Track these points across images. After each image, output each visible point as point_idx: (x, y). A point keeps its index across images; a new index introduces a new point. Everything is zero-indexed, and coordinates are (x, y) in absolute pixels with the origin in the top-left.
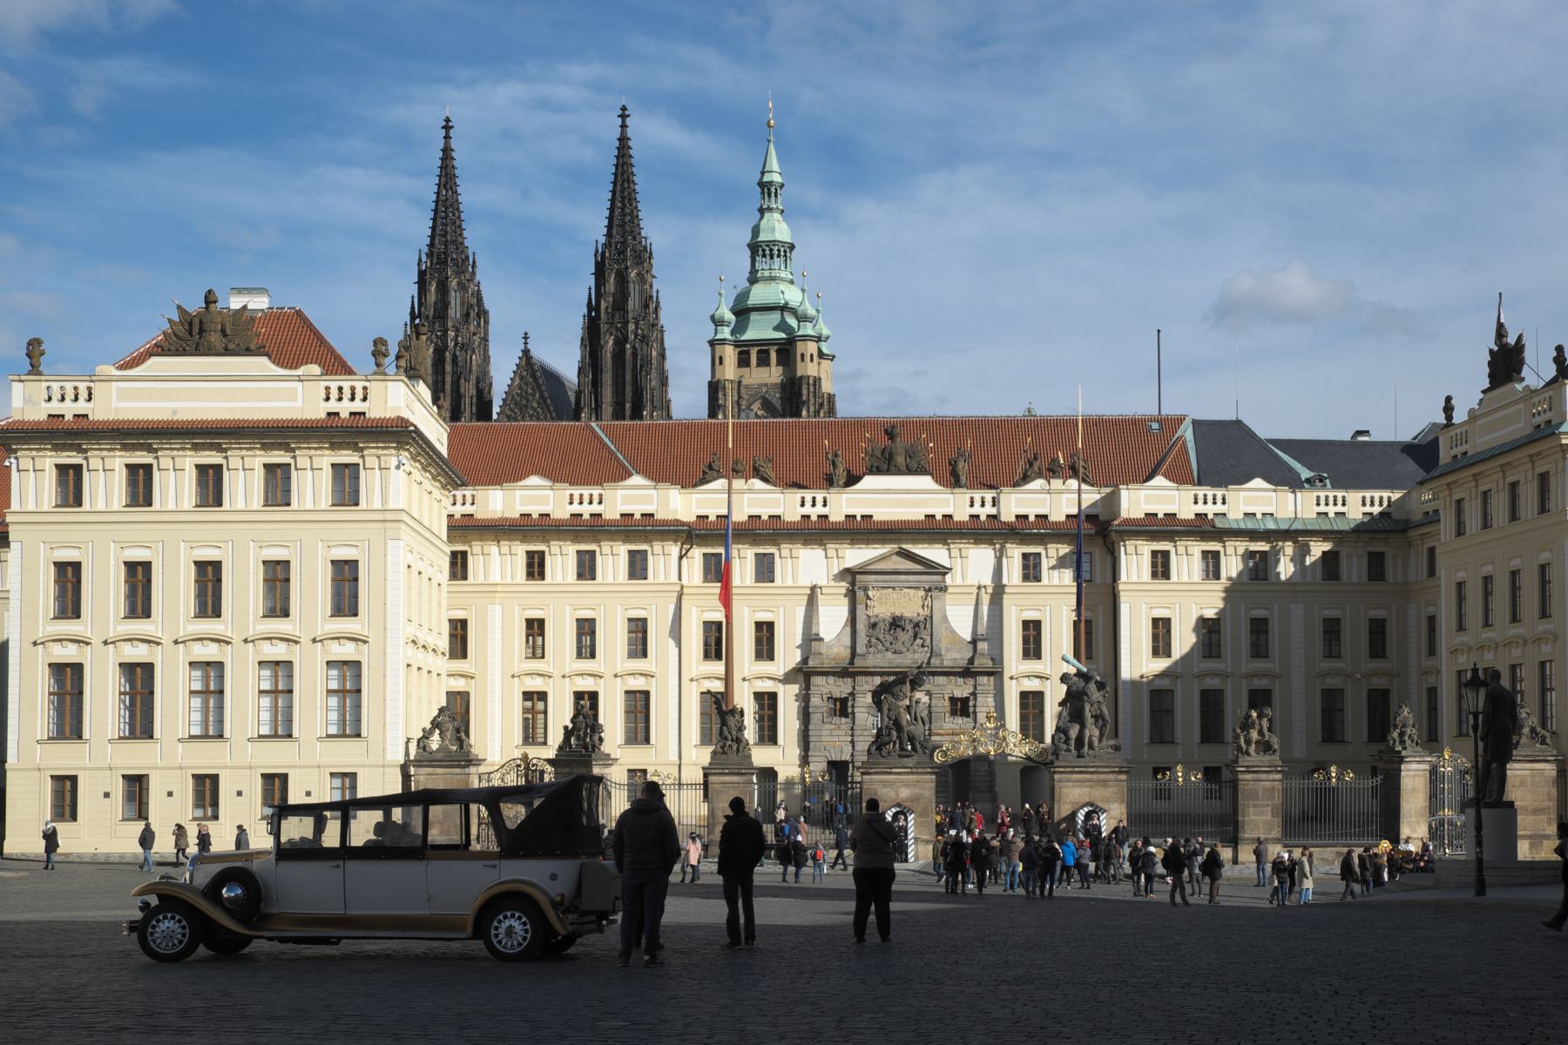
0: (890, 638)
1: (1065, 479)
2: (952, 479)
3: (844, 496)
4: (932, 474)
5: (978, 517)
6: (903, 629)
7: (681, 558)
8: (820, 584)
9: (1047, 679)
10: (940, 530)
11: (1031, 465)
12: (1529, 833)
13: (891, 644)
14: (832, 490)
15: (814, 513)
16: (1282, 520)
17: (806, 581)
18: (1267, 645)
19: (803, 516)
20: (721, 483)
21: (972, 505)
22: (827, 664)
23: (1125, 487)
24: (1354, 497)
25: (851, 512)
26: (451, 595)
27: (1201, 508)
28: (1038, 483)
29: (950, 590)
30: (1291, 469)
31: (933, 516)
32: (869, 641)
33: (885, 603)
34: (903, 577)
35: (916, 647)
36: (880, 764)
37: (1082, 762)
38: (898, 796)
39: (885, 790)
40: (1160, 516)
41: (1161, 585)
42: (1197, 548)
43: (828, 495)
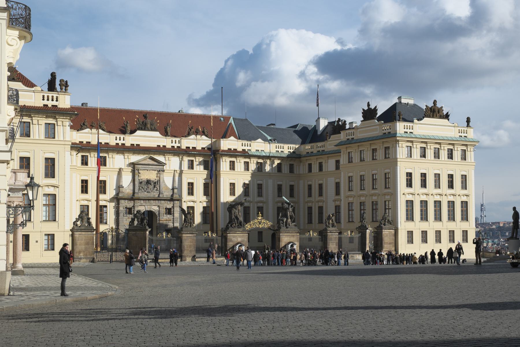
0: (146, 187)
1: (202, 135)
5: (174, 147)
6: (150, 184)
8: (122, 168)
9: (196, 202)
10: (162, 150)
11: (191, 130)
13: (146, 189)
14: (126, 135)
15: (120, 142)
16: (267, 152)
17: (118, 166)
18: (262, 192)
19: (116, 144)
21: (172, 143)
22: (126, 196)
23: (222, 139)
24: (286, 146)
26: (71, 169)
27: (244, 148)
28: (193, 136)
29: (165, 171)
30: (265, 136)
31: (160, 146)
32: (139, 188)
33: (147, 175)
34: (151, 166)
35: (154, 191)
37: (288, 229)
38: (237, 239)
39: (234, 239)
40: (232, 149)
41: (232, 172)
42: (243, 160)
43: (125, 137)
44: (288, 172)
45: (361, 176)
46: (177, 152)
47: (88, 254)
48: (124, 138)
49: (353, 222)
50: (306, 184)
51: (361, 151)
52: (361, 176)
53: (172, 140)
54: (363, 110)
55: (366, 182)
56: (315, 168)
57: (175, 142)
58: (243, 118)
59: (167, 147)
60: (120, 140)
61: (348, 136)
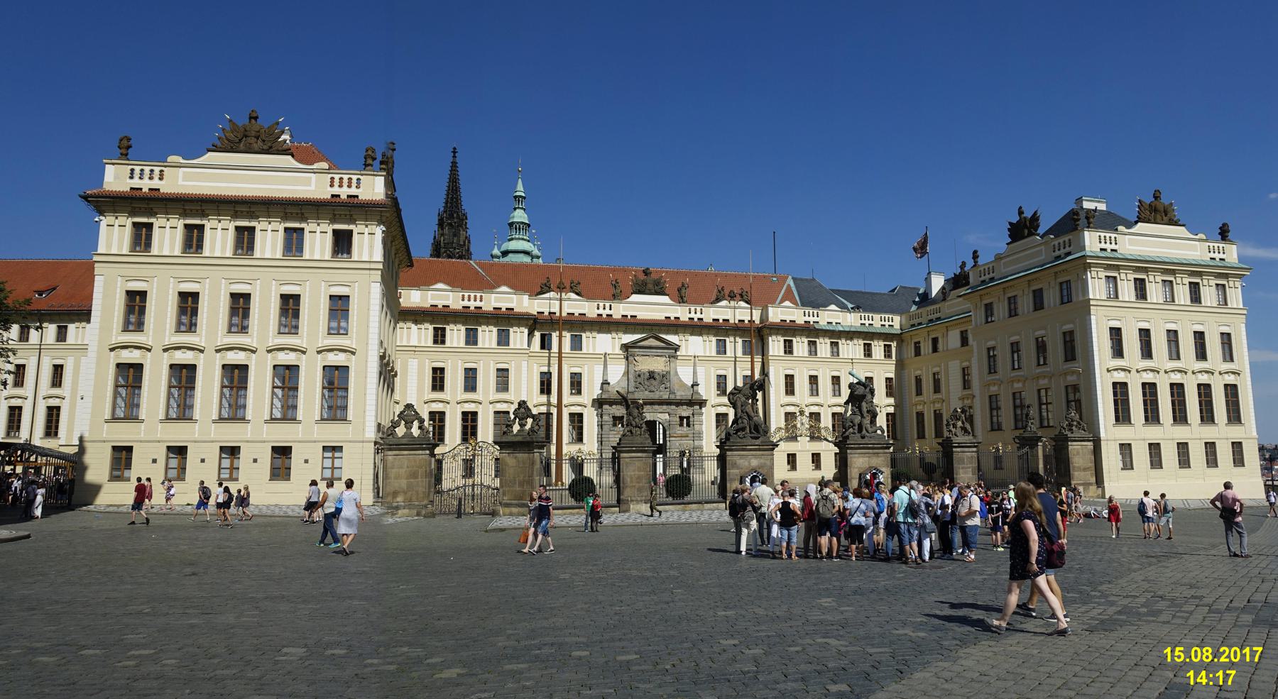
2: (681, 299)
8: (608, 352)
11: (720, 292)
12: (1082, 482)
15: (605, 313)
17: (600, 350)
19: (598, 315)
20: (552, 294)
21: (690, 313)
24: (877, 317)
25: (625, 313)
27: (807, 319)
28: (724, 303)
29: (679, 358)
30: (843, 303)
31: (670, 318)
36: (738, 443)
38: (749, 462)
39: (742, 461)
40: (788, 321)
41: (789, 357)
44: (883, 358)
45: (1012, 344)
46: (697, 328)
48: (611, 305)
49: (1001, 430)
51: (1009, 298)
52: (1012, 344)
53: (690, 309)
54: (1011, 224)
55: (1023, 353)
56: (926, 347)
59: (681, 319)
60: (604, 308)
61: (982, 275)
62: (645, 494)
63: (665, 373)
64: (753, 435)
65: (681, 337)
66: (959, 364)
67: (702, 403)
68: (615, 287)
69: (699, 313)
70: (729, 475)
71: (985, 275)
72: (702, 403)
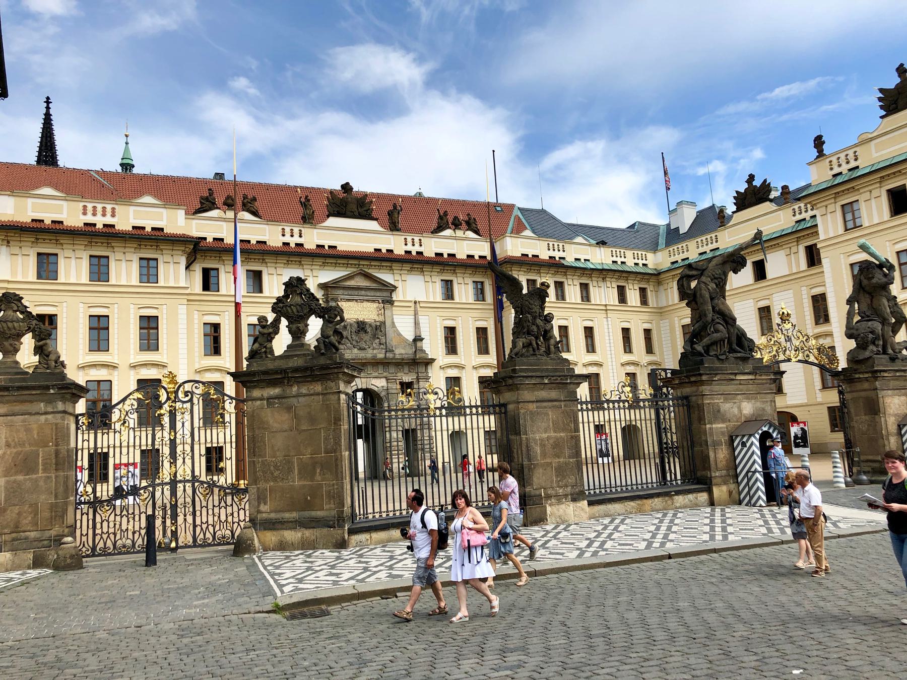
3: (315, 231)
4: (376, 219)
5: (410, 252)
6: (366, 332)
7: (186, 268)
9: (463, 368)
10: (387, 259)
15: (293, 241)
19: (284, 244)
20: (214, 213)
21: (406, 244)
24: (629, 254)
27: (552, 253)
28: (448, 232)
29: (396, 304)
31: (380, 250)
34: (363, 292)
35: (374, 345)
40: (530, 256)
44: (639, 304)
47: (26, 521)
50: (677, 325)
57: (413, 242)
58: (538, 207)
62: (571, 480)
63: (378, 324)
64: (739, 355)
65: (397, 277)
66: (752, 304)
67: (429, 362)
68: (305, 206)
69: (417, 244)
70: (712, 434)
71: (840, 166)
72: (429, 362)
